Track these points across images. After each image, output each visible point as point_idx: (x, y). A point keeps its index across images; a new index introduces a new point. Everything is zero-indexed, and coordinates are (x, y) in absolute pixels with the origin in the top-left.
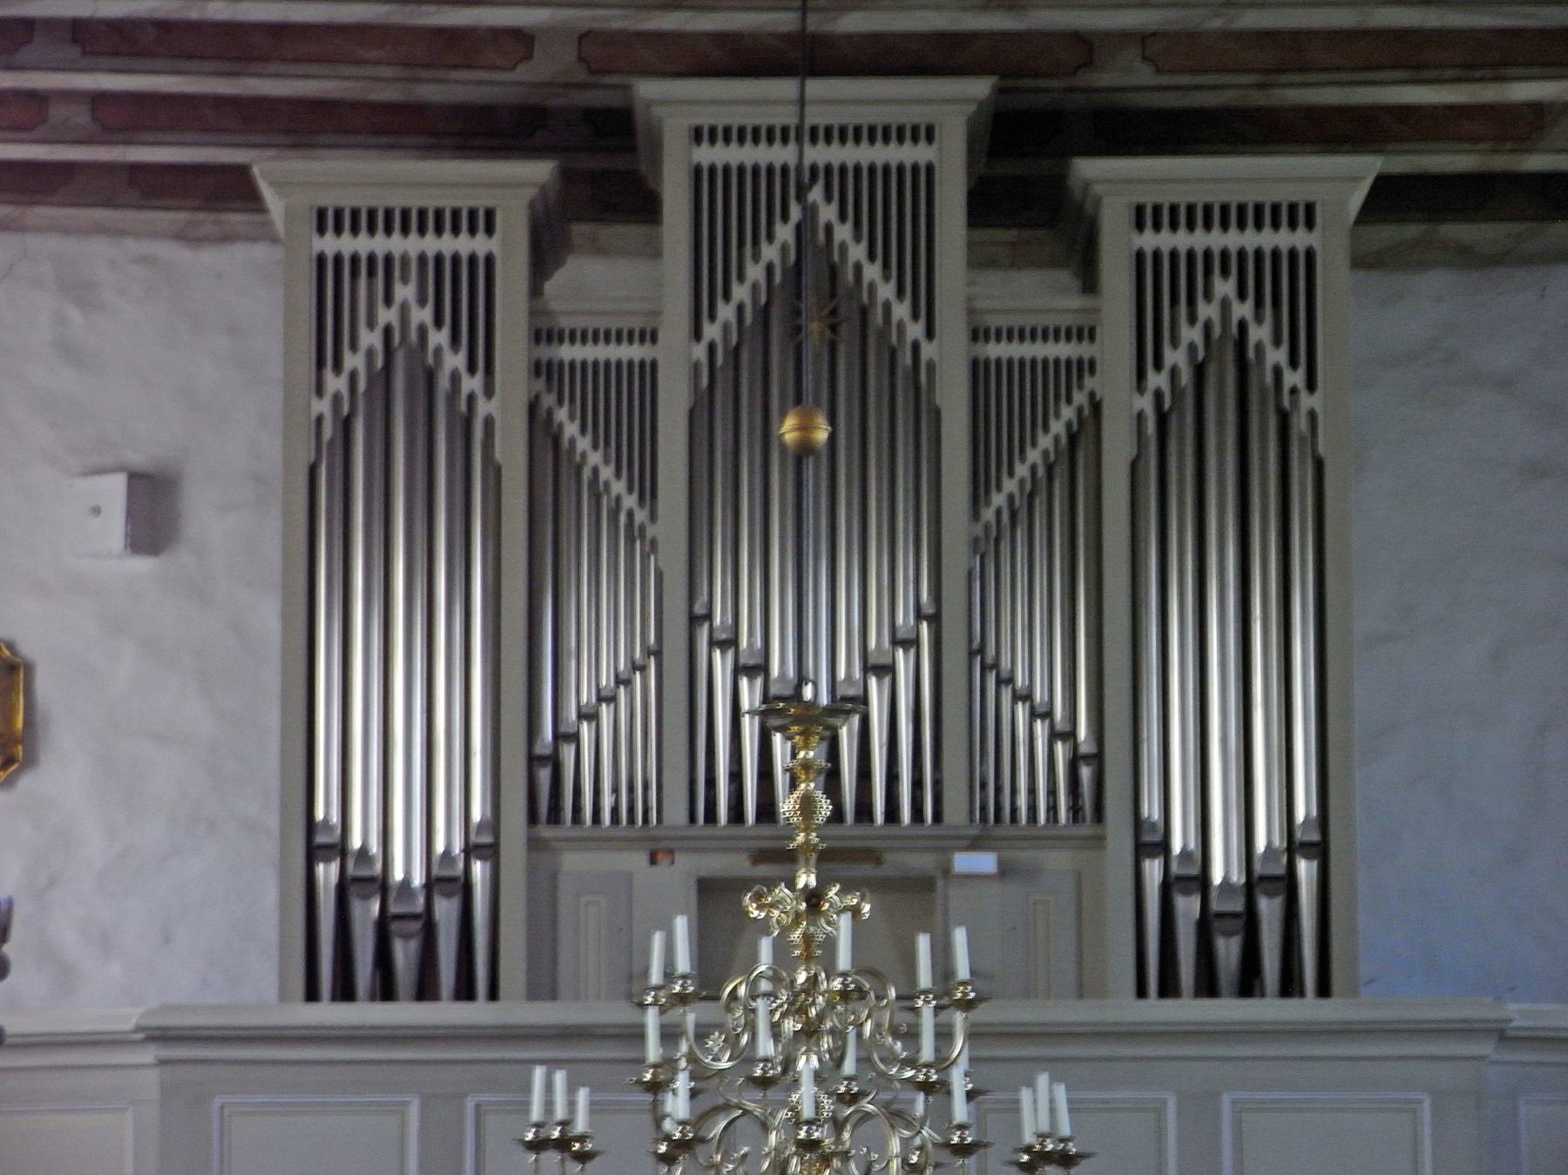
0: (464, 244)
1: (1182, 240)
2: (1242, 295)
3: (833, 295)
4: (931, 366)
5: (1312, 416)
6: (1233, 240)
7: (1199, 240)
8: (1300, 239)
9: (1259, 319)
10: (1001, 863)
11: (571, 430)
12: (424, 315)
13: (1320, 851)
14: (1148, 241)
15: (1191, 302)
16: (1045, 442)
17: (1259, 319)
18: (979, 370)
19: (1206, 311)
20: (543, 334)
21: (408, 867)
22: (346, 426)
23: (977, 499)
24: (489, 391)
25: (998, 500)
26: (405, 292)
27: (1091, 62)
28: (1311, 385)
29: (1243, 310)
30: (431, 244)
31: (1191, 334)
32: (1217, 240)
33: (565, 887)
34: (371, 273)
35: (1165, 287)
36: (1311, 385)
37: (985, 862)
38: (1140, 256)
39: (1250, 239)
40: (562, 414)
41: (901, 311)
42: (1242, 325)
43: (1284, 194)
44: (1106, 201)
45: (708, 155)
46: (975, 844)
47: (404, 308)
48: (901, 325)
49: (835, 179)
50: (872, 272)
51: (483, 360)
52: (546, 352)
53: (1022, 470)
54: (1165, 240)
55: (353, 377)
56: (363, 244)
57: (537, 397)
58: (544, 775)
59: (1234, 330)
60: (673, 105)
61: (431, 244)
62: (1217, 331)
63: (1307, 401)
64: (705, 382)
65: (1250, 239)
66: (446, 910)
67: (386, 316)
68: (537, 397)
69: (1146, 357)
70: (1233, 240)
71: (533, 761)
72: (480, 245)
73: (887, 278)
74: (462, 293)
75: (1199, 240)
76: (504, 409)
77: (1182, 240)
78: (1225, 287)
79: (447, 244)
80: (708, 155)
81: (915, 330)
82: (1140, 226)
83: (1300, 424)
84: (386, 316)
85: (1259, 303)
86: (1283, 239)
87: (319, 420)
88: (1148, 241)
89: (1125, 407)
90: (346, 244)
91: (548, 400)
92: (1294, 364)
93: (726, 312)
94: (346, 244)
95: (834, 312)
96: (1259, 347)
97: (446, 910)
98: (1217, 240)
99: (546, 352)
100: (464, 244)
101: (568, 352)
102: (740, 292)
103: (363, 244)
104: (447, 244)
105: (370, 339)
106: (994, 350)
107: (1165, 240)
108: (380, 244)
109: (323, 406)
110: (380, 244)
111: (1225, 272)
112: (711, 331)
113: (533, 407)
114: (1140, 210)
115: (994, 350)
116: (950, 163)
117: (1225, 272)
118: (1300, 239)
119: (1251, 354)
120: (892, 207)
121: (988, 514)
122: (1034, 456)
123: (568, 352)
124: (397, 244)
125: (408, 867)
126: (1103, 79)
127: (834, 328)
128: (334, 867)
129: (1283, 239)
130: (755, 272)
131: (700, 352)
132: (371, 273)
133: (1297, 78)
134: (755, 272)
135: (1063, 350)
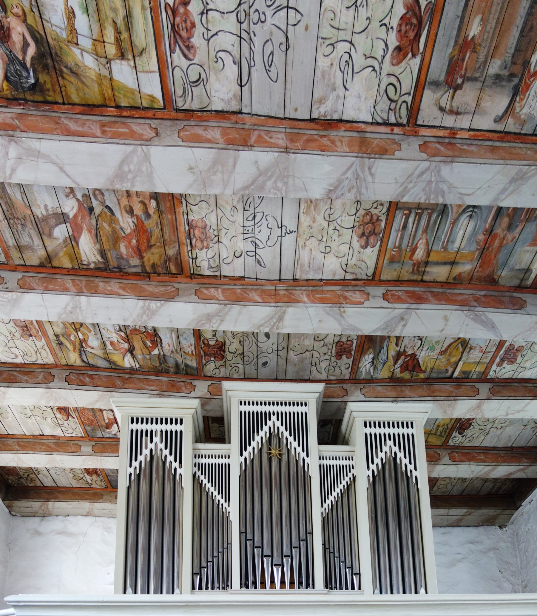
1: (377, 431)
6: (391, 431)
7: (382, 431)
14: (368, 430)
22: (139, 476)
24: (180, 467)
30: (164, 427)
32: (387, 431)
34: (147, 435)
35: (373, 444)
39: (396, 431)
47: (156, 444)
52: (197, 460)
54: (373, 430)
55: (141, 462)
61: (164, 427)
65: (396, 431)
67: (151, 446)
70: (391, 431)
75: (382, 431)
77: (377, 431)
84: (151, 446)
86: (405, 431)
87: (130, 474)
88: (368, 430)
90: (139, 427)
91: (199, 473)
94: (139, 427)
98: (387, 431)
99: (197, 460)
106: (325, 462)
107: (373, 430)
108: (149, 427)
109: (132, 470)
110: (149, 427)
111: (390, 439)
117: (390, 439)
123: (204, 461)
124: (154, 427)
129: (405, 431)
132: (147, 435)
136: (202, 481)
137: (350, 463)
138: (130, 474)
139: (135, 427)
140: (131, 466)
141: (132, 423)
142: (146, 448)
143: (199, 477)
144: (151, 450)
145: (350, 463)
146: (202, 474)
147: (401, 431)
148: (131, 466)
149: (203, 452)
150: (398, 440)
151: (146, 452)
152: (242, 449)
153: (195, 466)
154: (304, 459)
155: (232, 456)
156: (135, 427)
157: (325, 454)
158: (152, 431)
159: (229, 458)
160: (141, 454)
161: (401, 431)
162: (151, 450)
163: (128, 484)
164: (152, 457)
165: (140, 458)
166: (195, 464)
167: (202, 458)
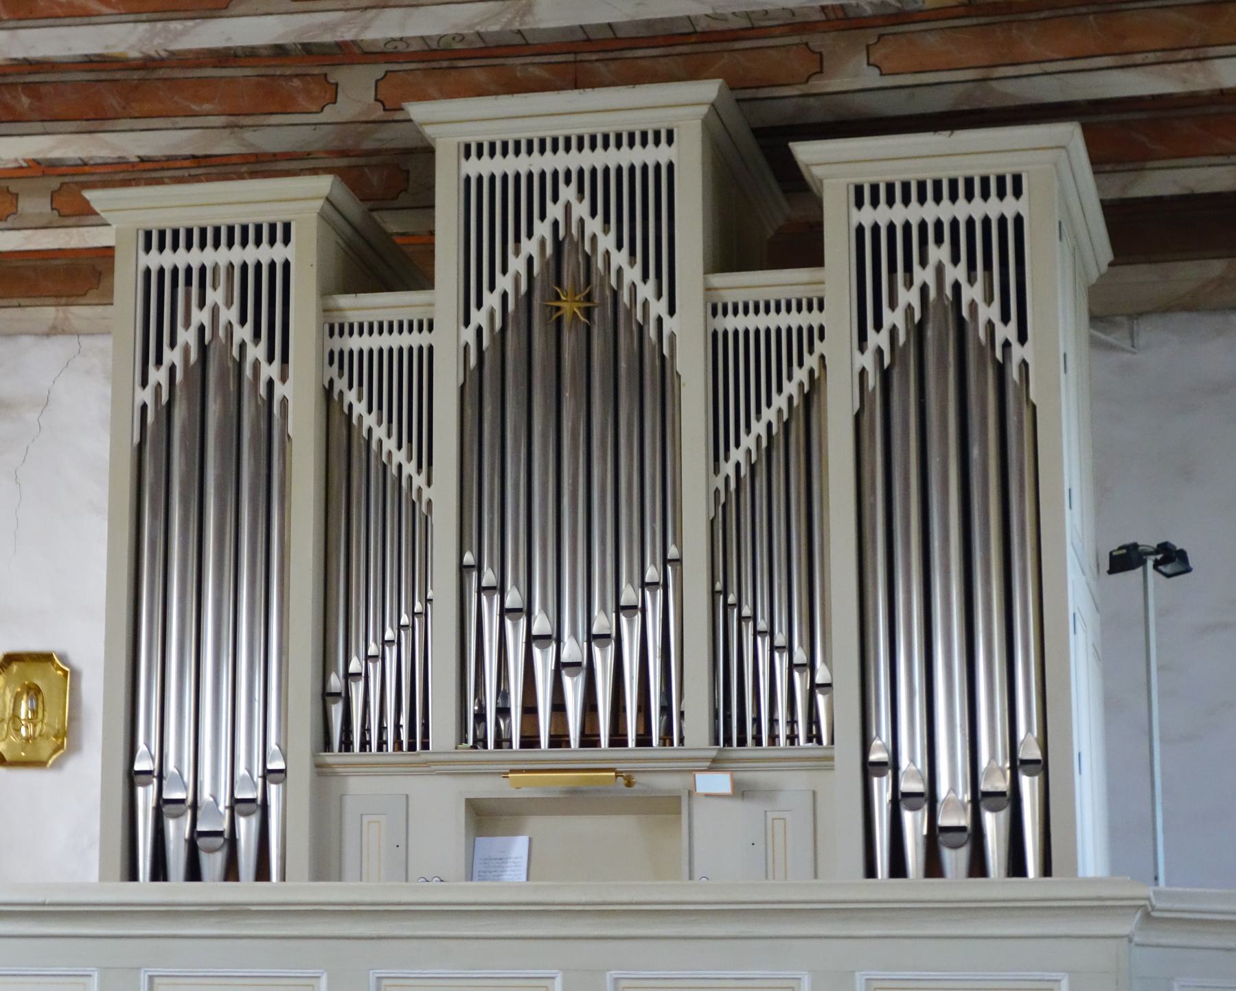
0: (266, 254)
1: (899, 214)
2: (955, 260)
3: (588, 281)
4: (672, 336)
5: (1024, 364)
6: (946, 211)
7: (914, 213)
8: (1010, 207)
9: (971, 280)
10: (736, 784)
11: (360, 408)
12: (230, 315)
13: (1041, 767)
14: (867, 216)
15: (908, 268)
16: (780, 401)
17: (971, 280)
18: (717, 341)
19: (923, 275)
20: (336, 329)
21: (215, 793)
23: (718, 454)
25: (737, 455)
26: (215, 296)
27: (821, 72)
28: (1022, 338)
29: (958, 273)
31: (909, 297)
32: (930, 212)
33: (352, 809)
34: (188, 282)
35: (885, 258)
36: (1022, 338)
37: (719, 782)
38: (860, 230)
39: (962, 210)
40: (351, 396)
41: (646, 291)
42: (957, 287)
43: (992, 167)
44: (825, 182)
45: (474, 167)
46: (715, 765)
48: (646, 304)
49: (586, 181)
50: (620, 258)
51: (280, 351)
52: (337, 343)
53: (759, 428)
54: (883, 215)
55: (172, 369)
56: (182, 258)
57: (331, 382)
58: (337, 711)
59: (948, 291)
60: (450, 123)
61: (237, 255)
62: (932, 294)
63: (1017, 352)
64: (473, 361)
65: (962, 210)
66: (246, 828)
67: (201, 317)
68: (331, 382)
69: (867, 317)
70: (946, 211)
71: (326, 696)
72: (278, 253)
73: (632, 263)
74: (263, 295)
75: (914, 213)
76: (299, 397)
77: (899, 214)
78: (939, 253)
79: (251, 255)
80: (474, 167)
81: (659, 307)
82: (859, 204)
83: (1014, 373)
84: (201, 317)
85: (971, 266)
86: (993, 208)
87: (144, 407)
88: (867, 216)
89: (845, 365)
90: (168, 259)
91: (341, 384)
92: (1005, 319)
93: (492, 300)
94: (168, 259)
95: (589, 298)
96: (973, 305)
97: (246, 828)
98: (930, 212)
99: (337, 343)
100: (266, 254)
101: (356, 343)
102: (504, 283)
103: (182, 258)
104: (251, 255)
105: (187, 336)
106: (731, 323)
107: (883, 215)
108: (195, 258)
109: (147, 395)
110: (195, 258)
111: (939, 240)
112: (479, 317)
113: (328, 392)
114: (859, 190)
115: (731, 323)
116: (688, 161)
117: (939, 240)
118: (1010, 207)
119: (965, 313)
120: (636, 201)
121: (728, 468)
122: (769, 414)
123: (356, 343)
124: (209, 257)
125: (215, 793)
126: (834, 83)
127: (588, 313)
128: (152, 789)
129: (993, 208)
130: (517, 264)
131: (469, 335)
132: (188, 282)
133: (1011, 71)
134: (517, 264)
135: (795, 320)
136: (350, 406)
137: (815, 318)
138: (144, 407)
139: (154, 260)
140: (144, 383)
141: (148, 248)
142: (187, 324)
143: (341, 393)
144: (202, 329)
145: (815, 318)
146: (350, 387)
147: (978, 209)
148: (144, 383)
149: (354, 317)
150: (972, 243)
151: (187, 336)
152: (469, 301)
153: (331, 362)
154: (660, 320)
155: (442, 323)
156: (154, 260)
157: (730, 297)
158: (203, 269)
159: (431, 329)
160: (173, 345)
161: (978, 209)
162: (202, 329)
163: (136, 439)
164: (203, 349)
165: (172, 356)
166: (332, 353)
167: (351, 334)
